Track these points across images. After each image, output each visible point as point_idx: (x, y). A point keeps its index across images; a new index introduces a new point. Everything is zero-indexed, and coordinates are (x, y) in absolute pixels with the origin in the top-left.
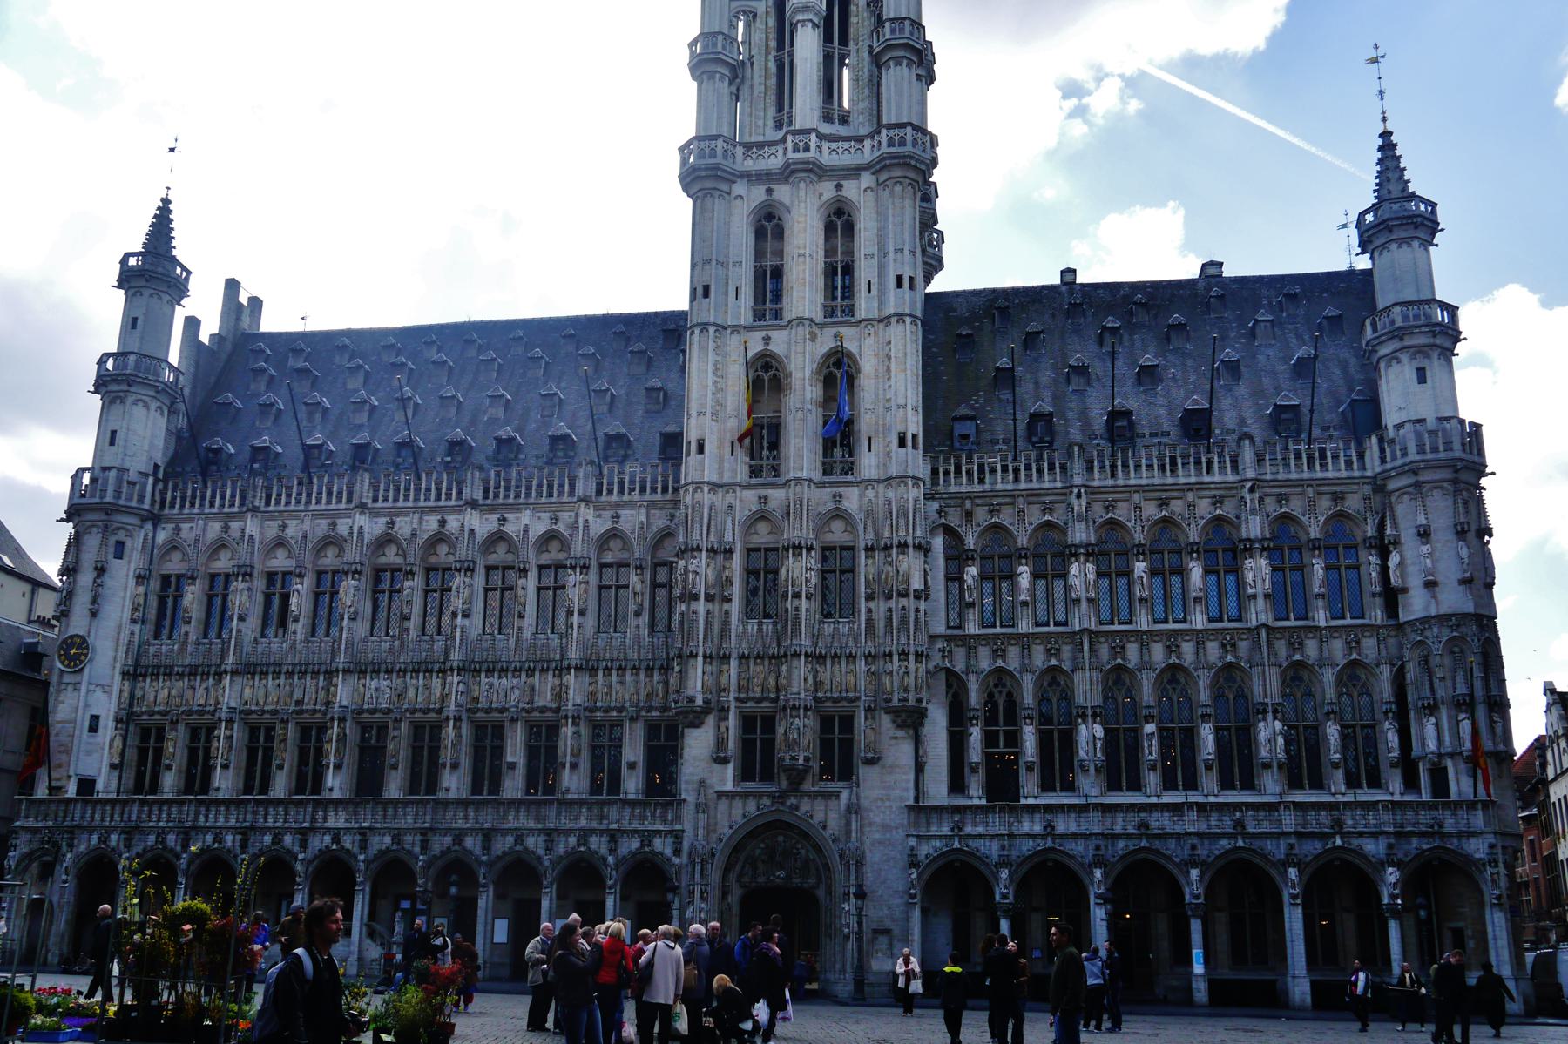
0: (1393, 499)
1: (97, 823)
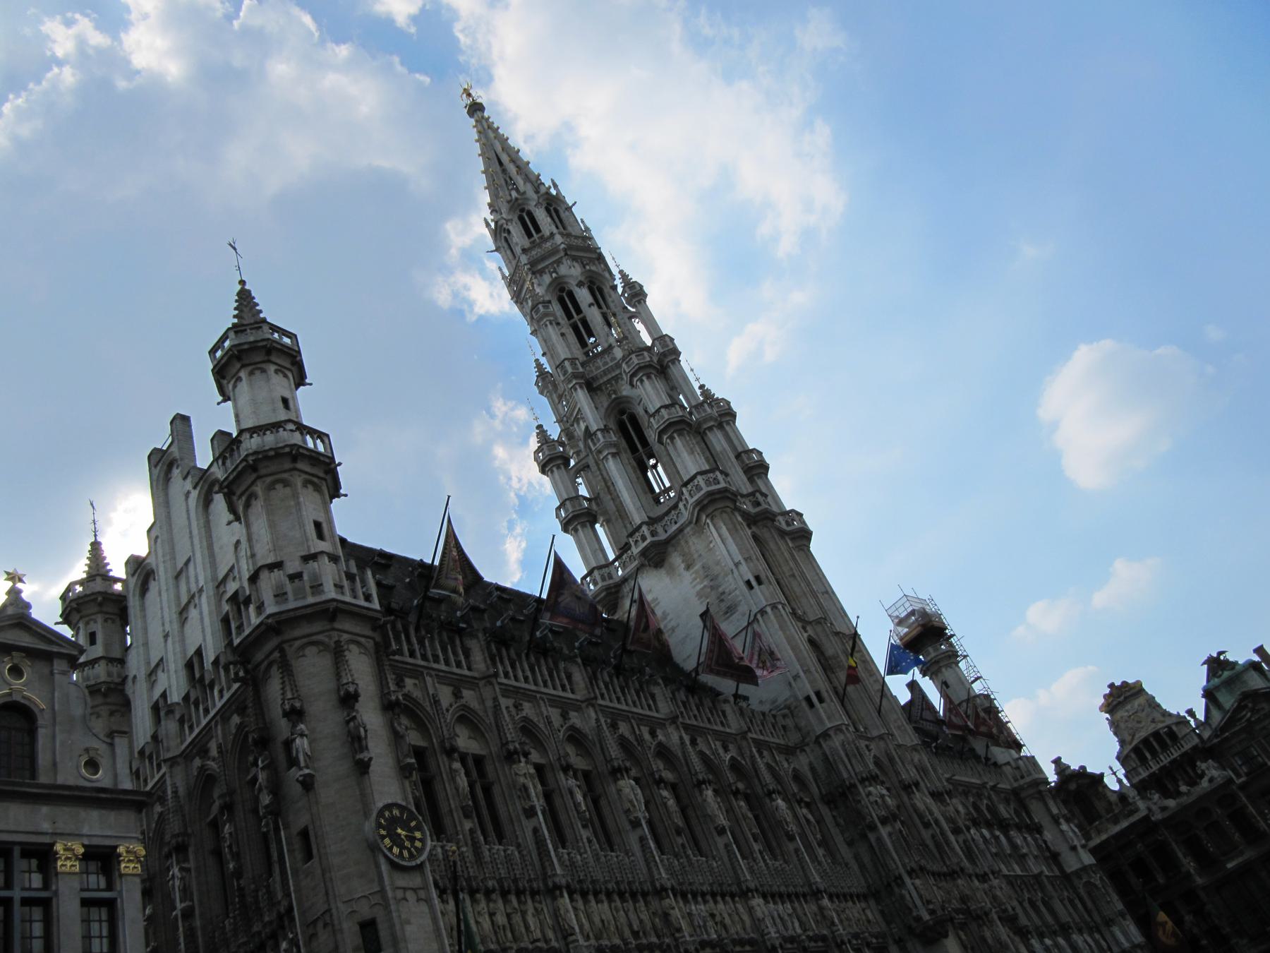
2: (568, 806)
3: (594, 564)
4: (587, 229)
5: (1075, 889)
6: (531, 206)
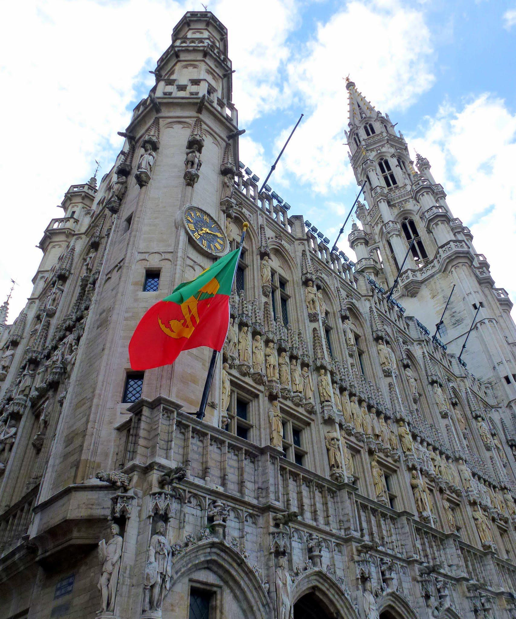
2: (341, 340)
4: (401, 135)
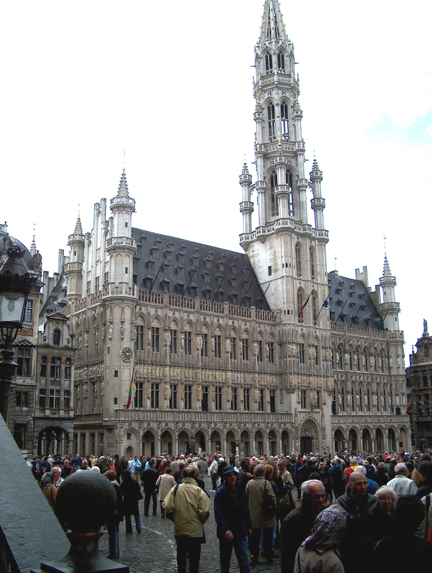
0: (391, 347)
1: (146, 419)
3: (245, 232)
5: (391, 380)
6: (272, 53)
